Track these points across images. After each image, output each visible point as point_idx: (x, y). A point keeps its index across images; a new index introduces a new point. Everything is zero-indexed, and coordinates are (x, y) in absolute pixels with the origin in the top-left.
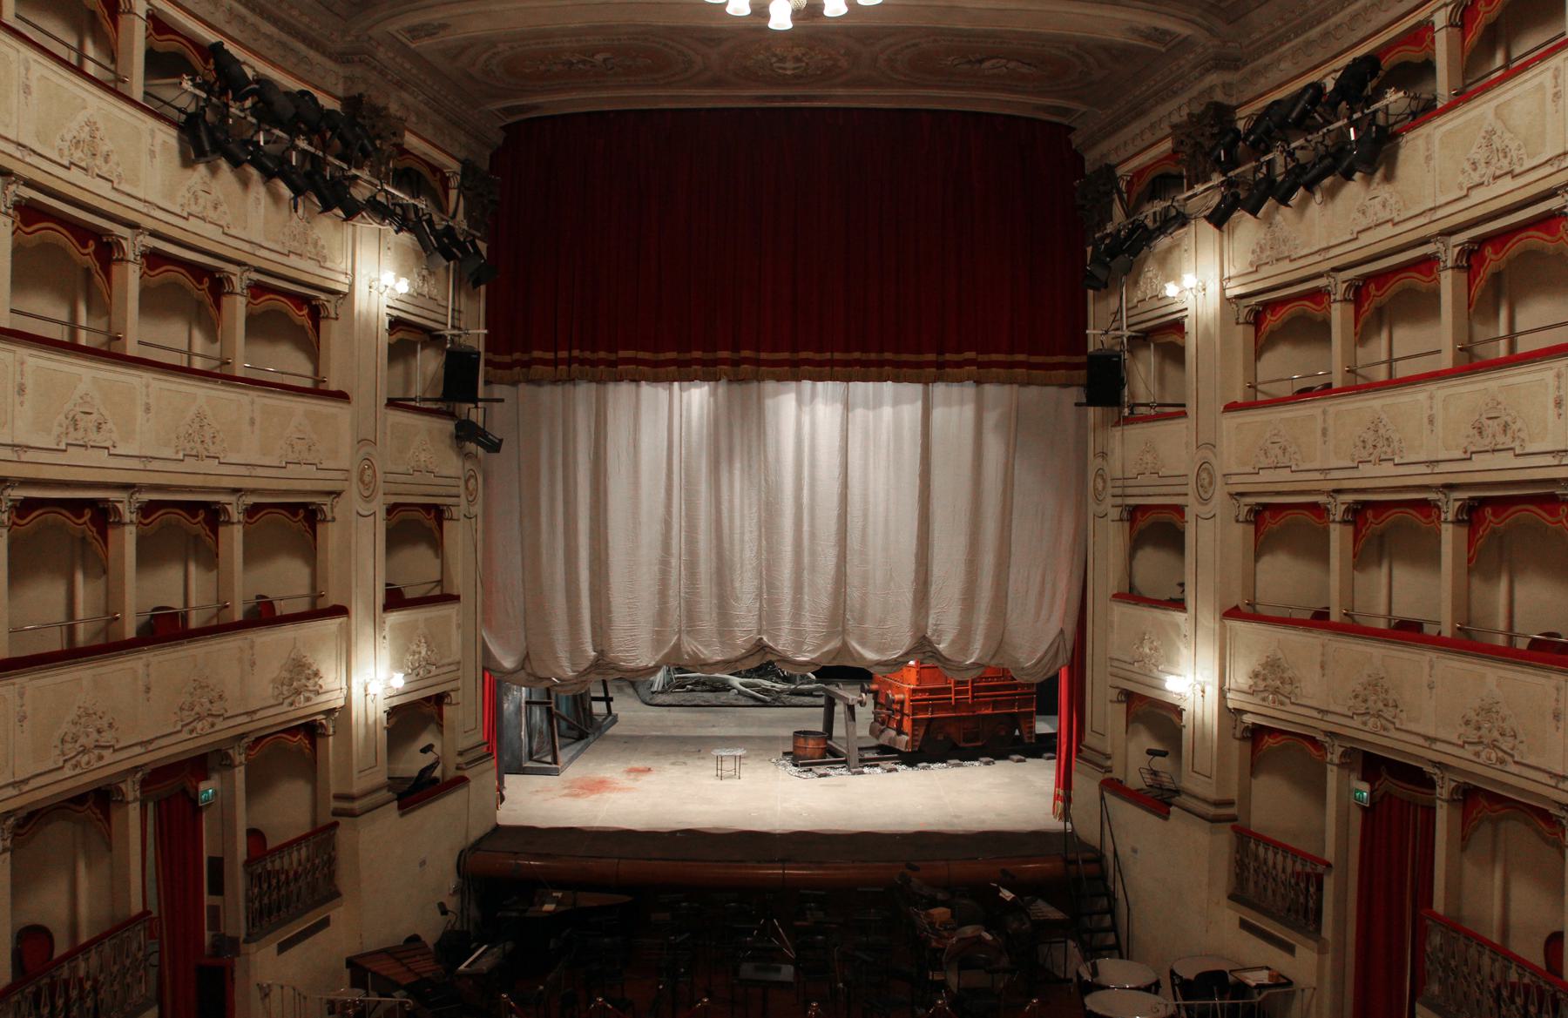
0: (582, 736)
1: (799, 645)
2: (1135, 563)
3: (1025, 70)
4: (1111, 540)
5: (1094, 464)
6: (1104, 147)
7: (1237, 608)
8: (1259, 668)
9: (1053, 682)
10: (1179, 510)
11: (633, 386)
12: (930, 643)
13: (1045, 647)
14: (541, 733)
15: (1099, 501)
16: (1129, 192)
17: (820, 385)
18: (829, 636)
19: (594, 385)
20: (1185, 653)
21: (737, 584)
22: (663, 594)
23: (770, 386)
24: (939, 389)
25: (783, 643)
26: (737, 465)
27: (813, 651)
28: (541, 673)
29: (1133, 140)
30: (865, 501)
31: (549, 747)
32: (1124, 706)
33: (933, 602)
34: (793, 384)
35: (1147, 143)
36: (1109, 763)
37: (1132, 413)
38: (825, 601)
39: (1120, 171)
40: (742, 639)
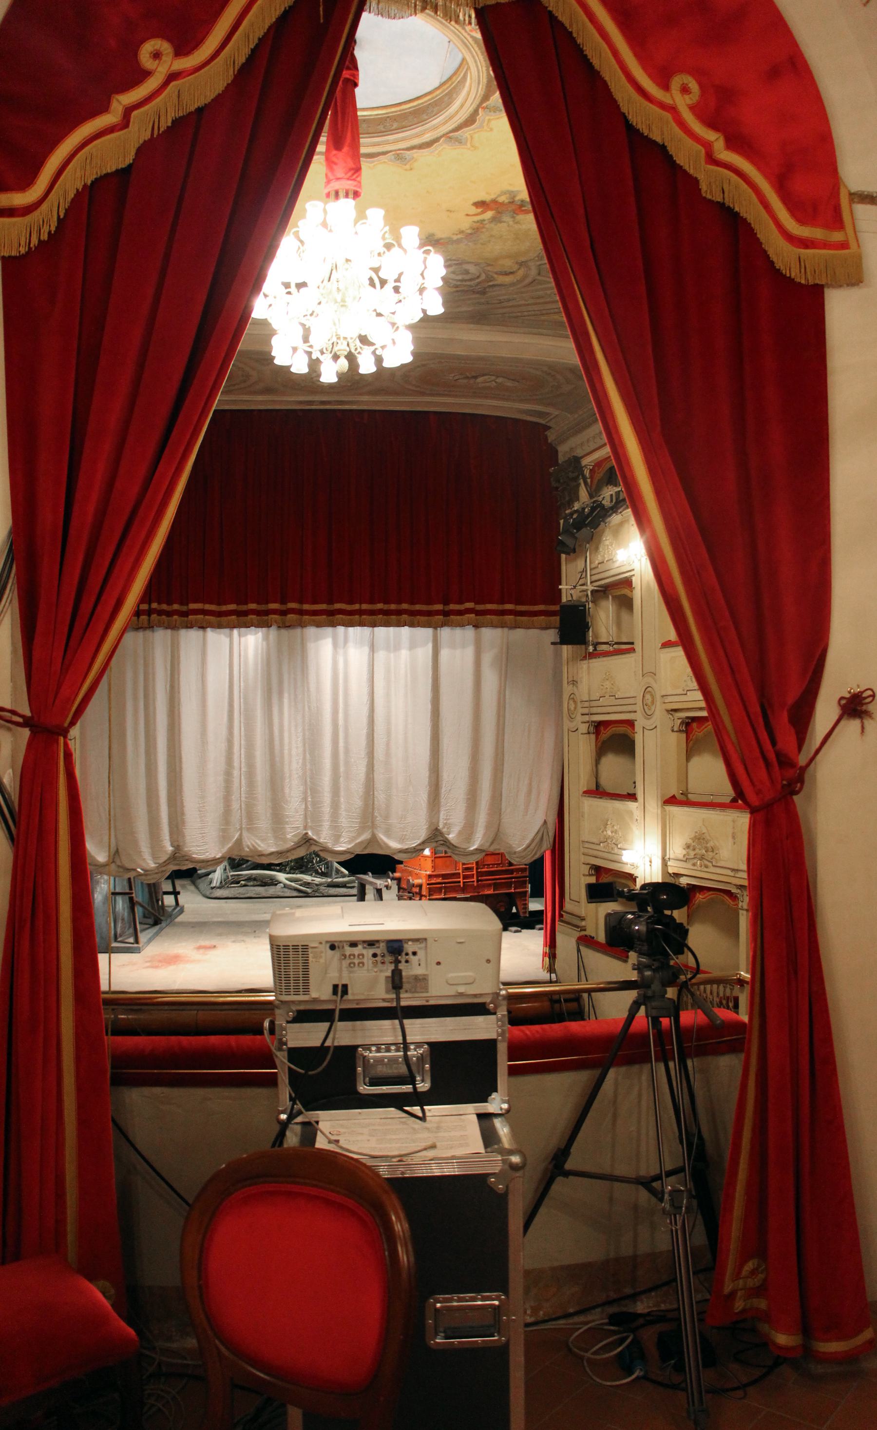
0: (157, 922)
1: (337, 839)
2: (600, 767)
3: (509, 384)
4: (582, 748)
5: (567, 689)
6: (573, 442)
7: (674, 797)
8: (690, 841)
9: (540, 862)
10: (631, 723)
11: (200, 633)
12: (441, 834)
13: (531, 836)
14: (123, 919)
15: (571, 719)
16: (592, 477)
17: (351, 629)
18: (362, 829)
19: (169, 631)
20: (636, 832)
21: (287, 791)
22: (227, 799)
23: (311, 631)
24: (445, 633)
25: (324, 837)
26: (286, 695)
27: (350, 842)
28: (128, 865)
29: (594, 437)
30: (388, 722)
31: (131, 930)
33: (443, 801)
34: (329, 630)
35: (596, 446)
36: (583, 923)
37: (595, 649)
38: (358, 803)
39: (584, 462)
40: (291, 835)
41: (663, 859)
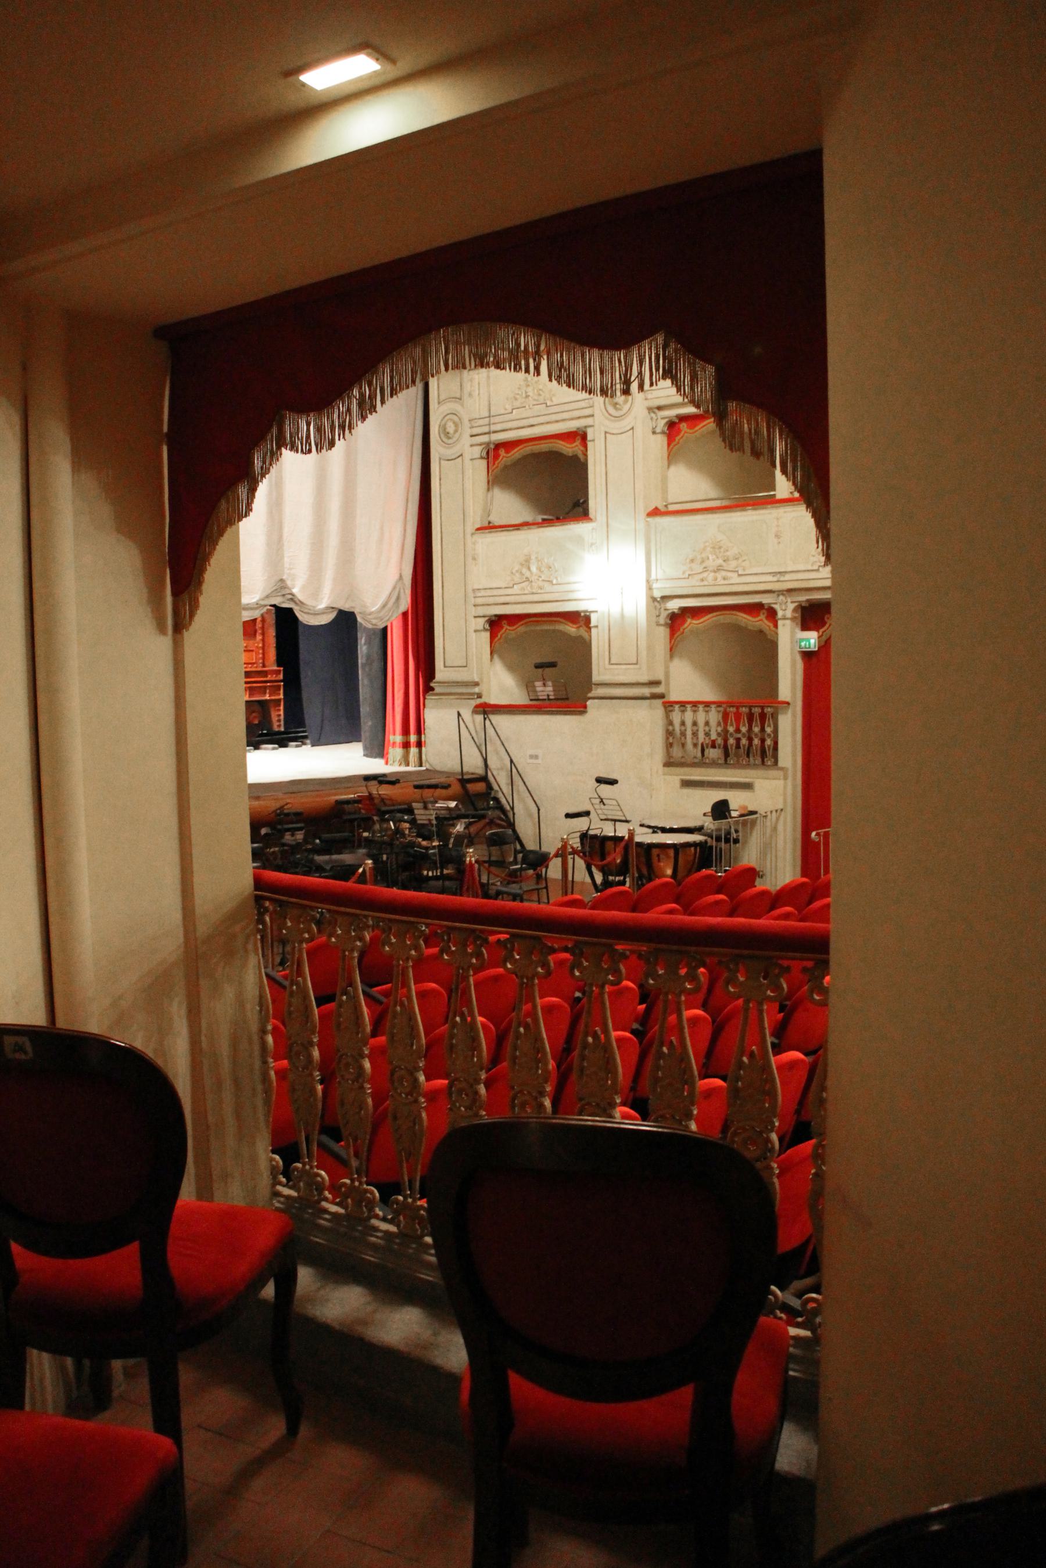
7: (656, 508)
13: (386, 593)
32: (488, 634)
41: (648, 581)
